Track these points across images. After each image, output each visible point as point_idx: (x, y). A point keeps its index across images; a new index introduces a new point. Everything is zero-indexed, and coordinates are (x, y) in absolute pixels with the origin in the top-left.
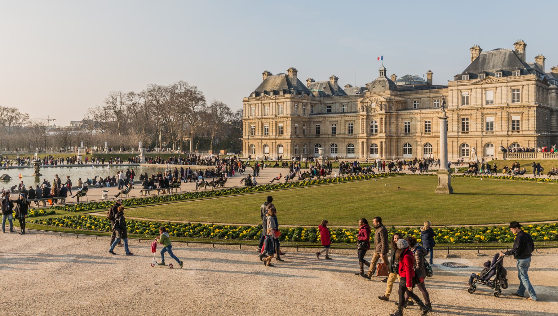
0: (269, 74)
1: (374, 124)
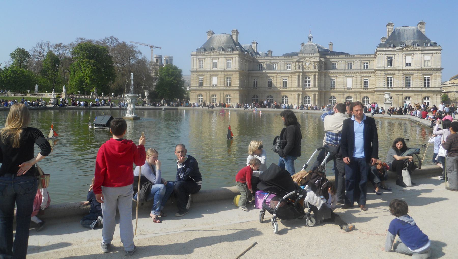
0: (213, 33)
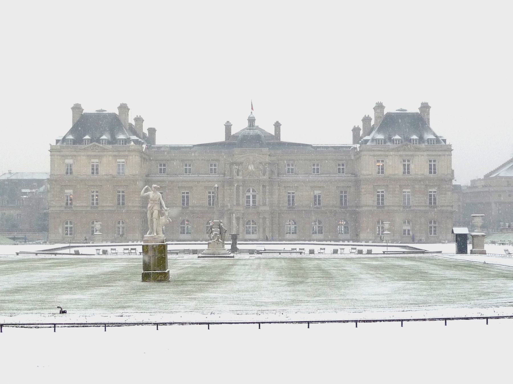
1: (251, 194)
